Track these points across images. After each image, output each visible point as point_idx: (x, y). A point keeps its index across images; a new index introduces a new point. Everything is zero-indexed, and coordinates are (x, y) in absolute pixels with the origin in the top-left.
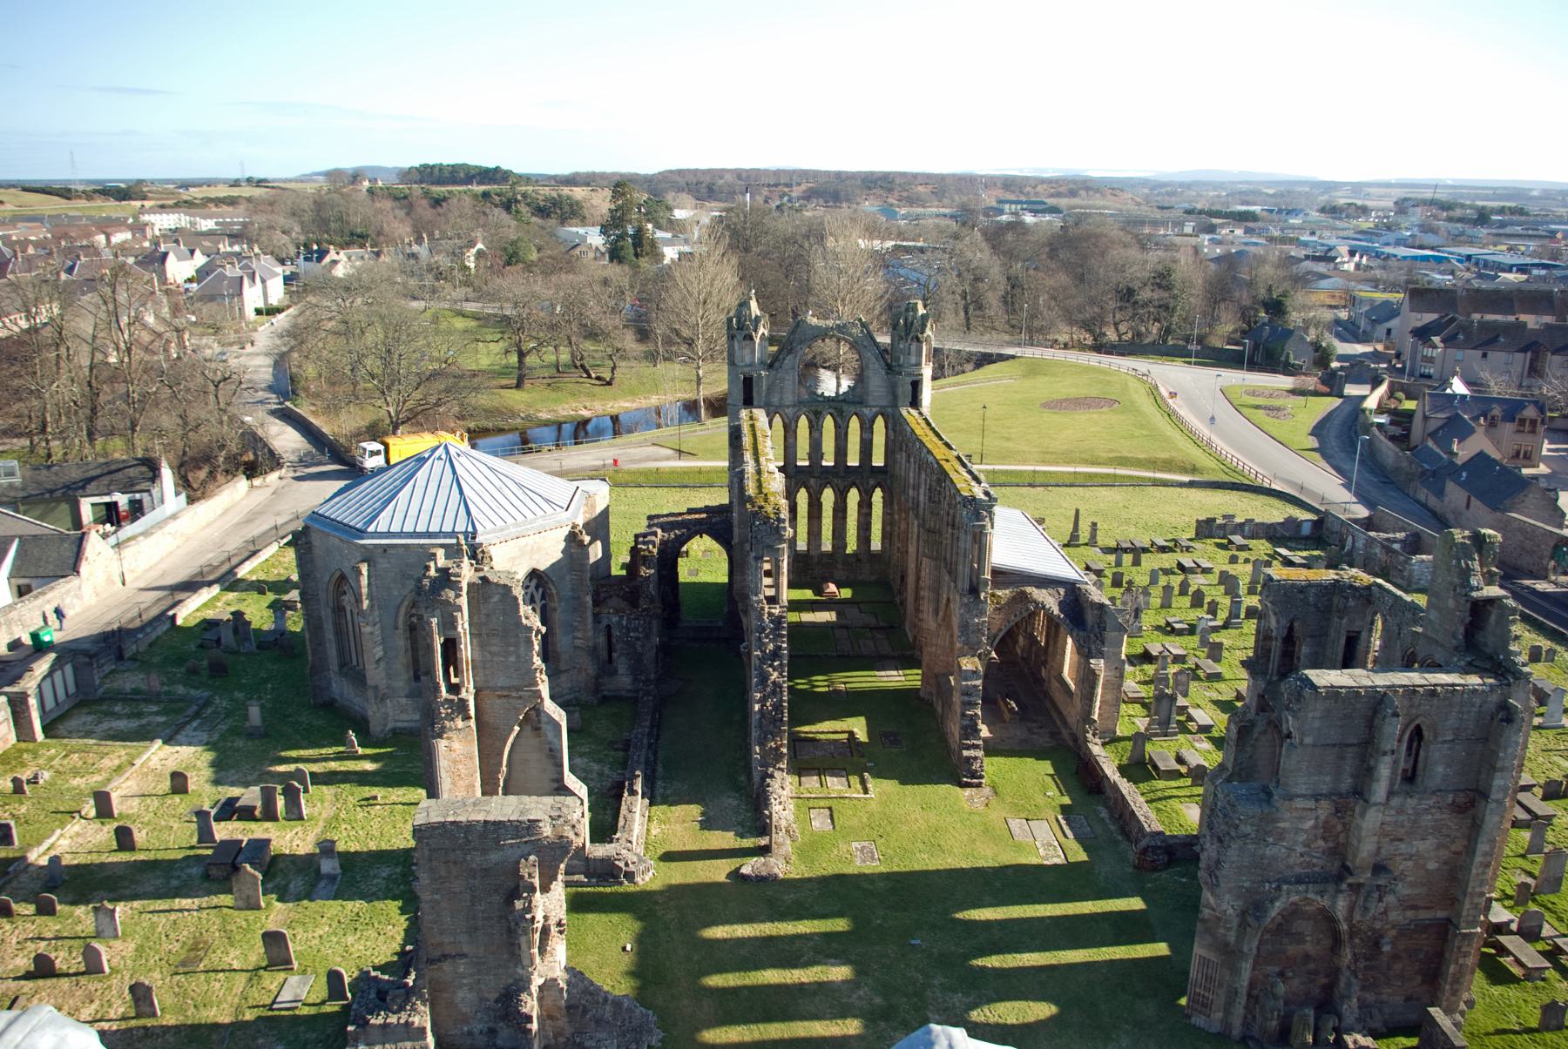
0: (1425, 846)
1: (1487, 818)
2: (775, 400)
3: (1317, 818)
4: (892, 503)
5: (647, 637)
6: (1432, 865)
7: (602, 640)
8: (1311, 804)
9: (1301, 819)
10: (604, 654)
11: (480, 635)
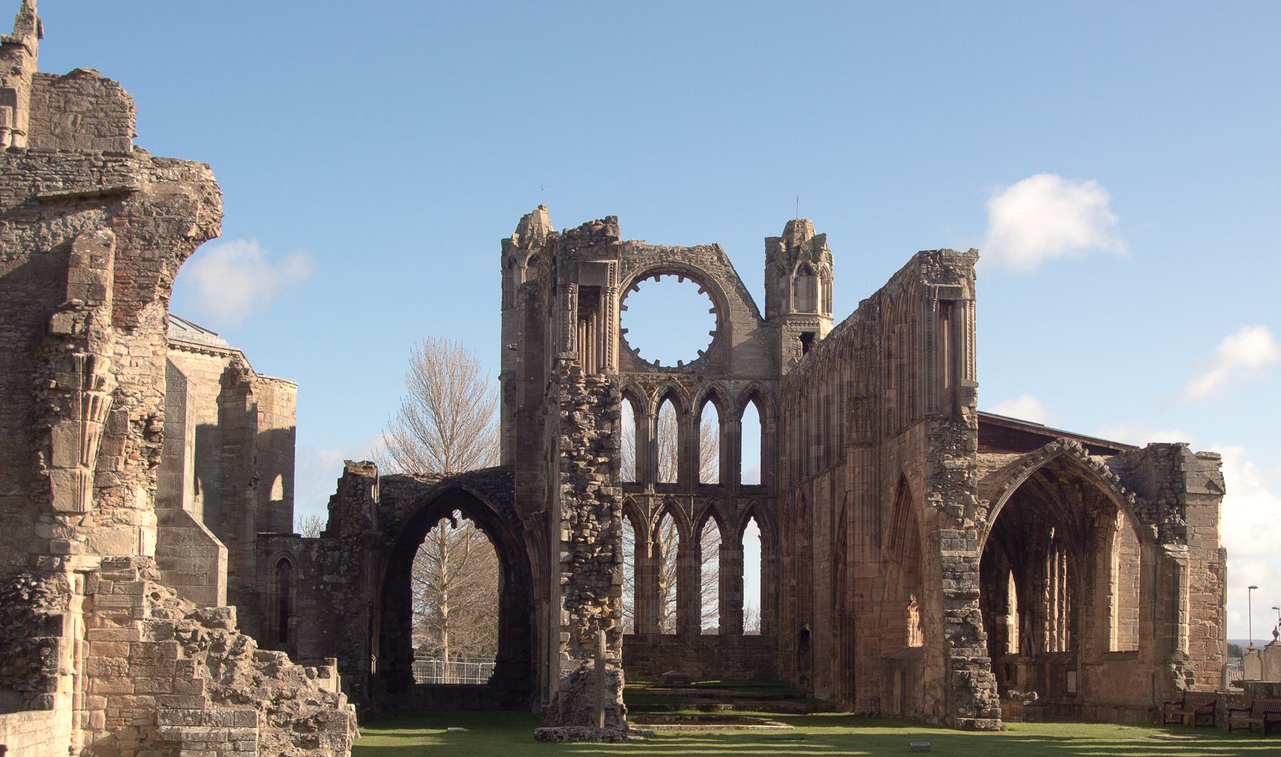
4: (776, 542)
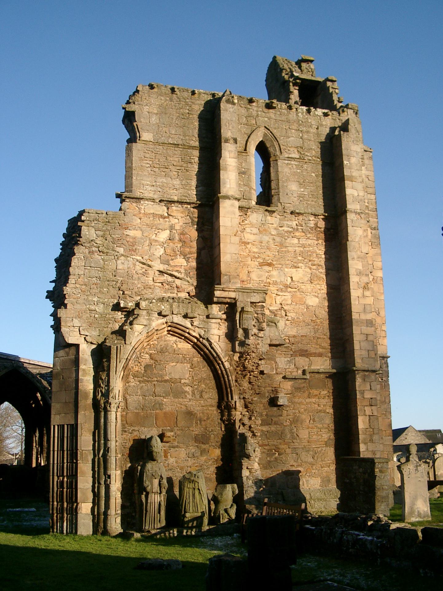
3: (172, 228)
8: (162, 210)
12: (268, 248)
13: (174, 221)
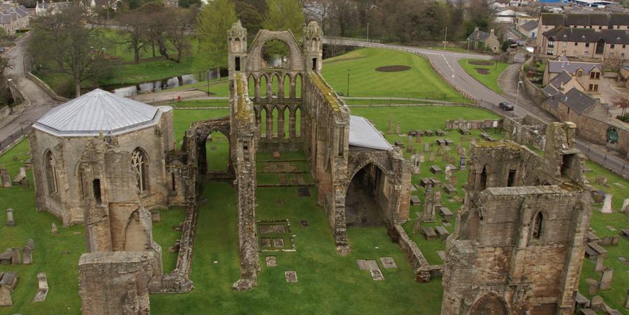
0: (545, 268)
1: (573, 254)
2: (250, 68)
5: (192, 178)
6: (548, 276)
7: (170, 179)
8: (493, 249)
9: (488, 257)
10: (171, 186)
11: (111, 178)
12: (534, 259)
13: (496, 253)
